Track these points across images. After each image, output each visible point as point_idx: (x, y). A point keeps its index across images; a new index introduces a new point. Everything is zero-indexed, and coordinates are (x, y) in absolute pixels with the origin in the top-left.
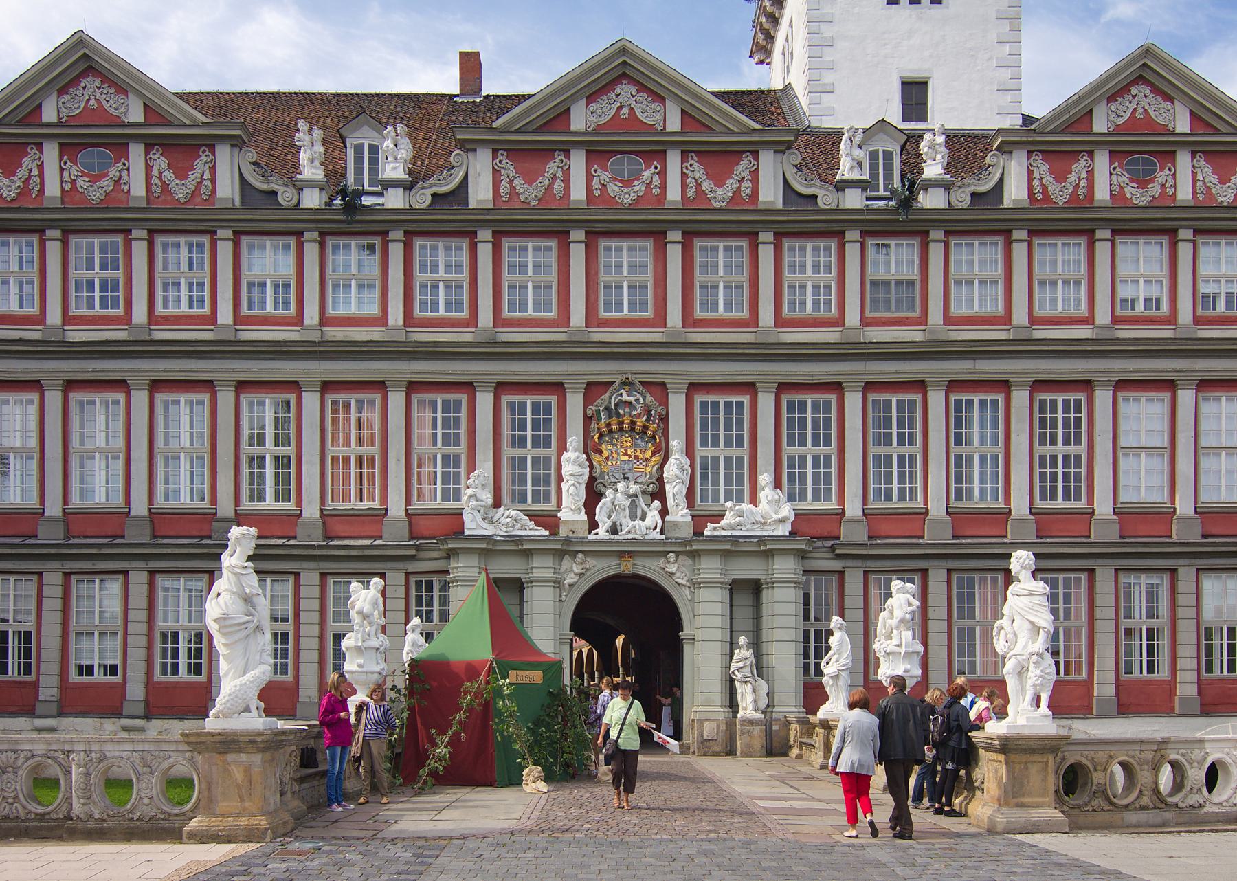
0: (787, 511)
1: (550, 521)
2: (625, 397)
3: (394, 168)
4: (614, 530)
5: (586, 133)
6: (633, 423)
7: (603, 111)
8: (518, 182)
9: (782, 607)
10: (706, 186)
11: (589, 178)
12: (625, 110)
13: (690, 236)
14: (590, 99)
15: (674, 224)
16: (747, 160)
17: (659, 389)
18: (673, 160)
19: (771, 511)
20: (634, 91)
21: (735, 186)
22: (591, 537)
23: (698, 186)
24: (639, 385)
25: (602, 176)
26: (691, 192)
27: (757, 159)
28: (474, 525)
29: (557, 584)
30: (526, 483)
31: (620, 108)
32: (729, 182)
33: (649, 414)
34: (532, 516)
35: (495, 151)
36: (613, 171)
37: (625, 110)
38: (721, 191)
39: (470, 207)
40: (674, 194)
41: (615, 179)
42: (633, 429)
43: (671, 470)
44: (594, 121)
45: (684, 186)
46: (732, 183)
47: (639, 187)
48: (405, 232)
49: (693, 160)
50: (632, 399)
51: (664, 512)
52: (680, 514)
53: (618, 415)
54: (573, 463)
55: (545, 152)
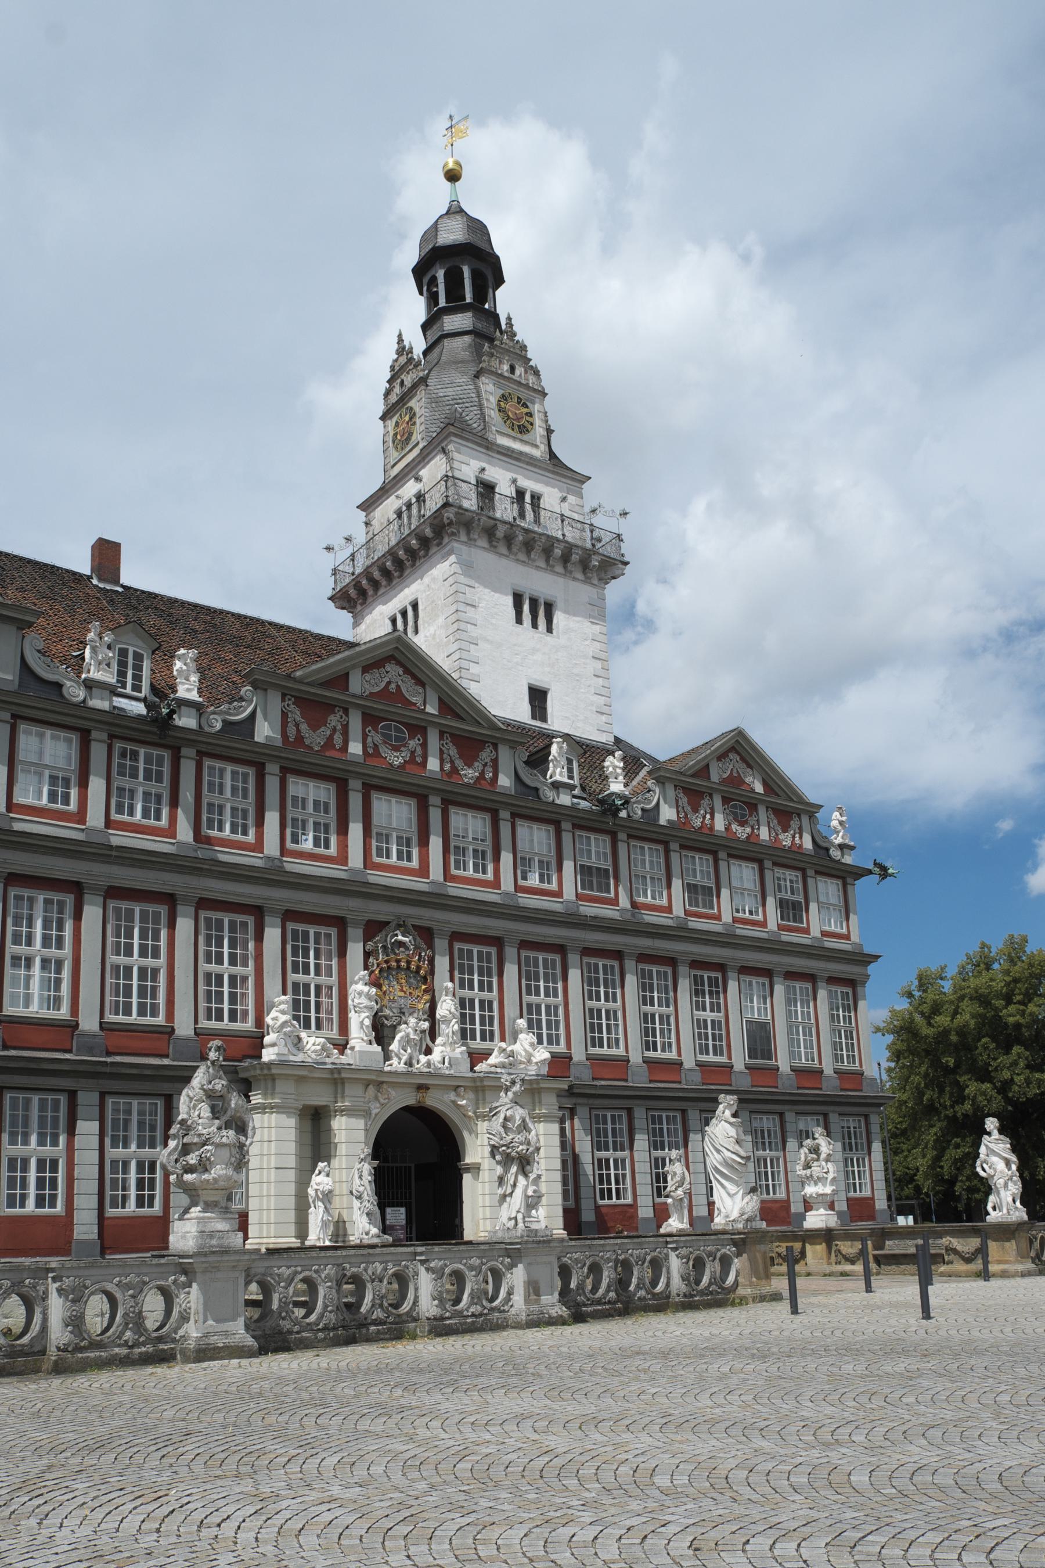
0: (542, 1054)
2: (400, 937)
3: (188, 690)
6: (408, 963)
8: (304, 727)
10: (459, 763)
13: (447, 803)
14: (366, 669)
15: (437, 791)
19: (529, 1051)
20: (401, 673)
22: (387, 1069)
26: (447, 767)
31: (389, 683)
32: (476, 764)
33: (420, 956)
35: (284, 696)
36: (383, 734)
37: (393, 686)
39: (256, 739)
41: (385, 742)
42: (408, 968)
48: (198, 751)
53: (395, 954)
55: (329, 707)
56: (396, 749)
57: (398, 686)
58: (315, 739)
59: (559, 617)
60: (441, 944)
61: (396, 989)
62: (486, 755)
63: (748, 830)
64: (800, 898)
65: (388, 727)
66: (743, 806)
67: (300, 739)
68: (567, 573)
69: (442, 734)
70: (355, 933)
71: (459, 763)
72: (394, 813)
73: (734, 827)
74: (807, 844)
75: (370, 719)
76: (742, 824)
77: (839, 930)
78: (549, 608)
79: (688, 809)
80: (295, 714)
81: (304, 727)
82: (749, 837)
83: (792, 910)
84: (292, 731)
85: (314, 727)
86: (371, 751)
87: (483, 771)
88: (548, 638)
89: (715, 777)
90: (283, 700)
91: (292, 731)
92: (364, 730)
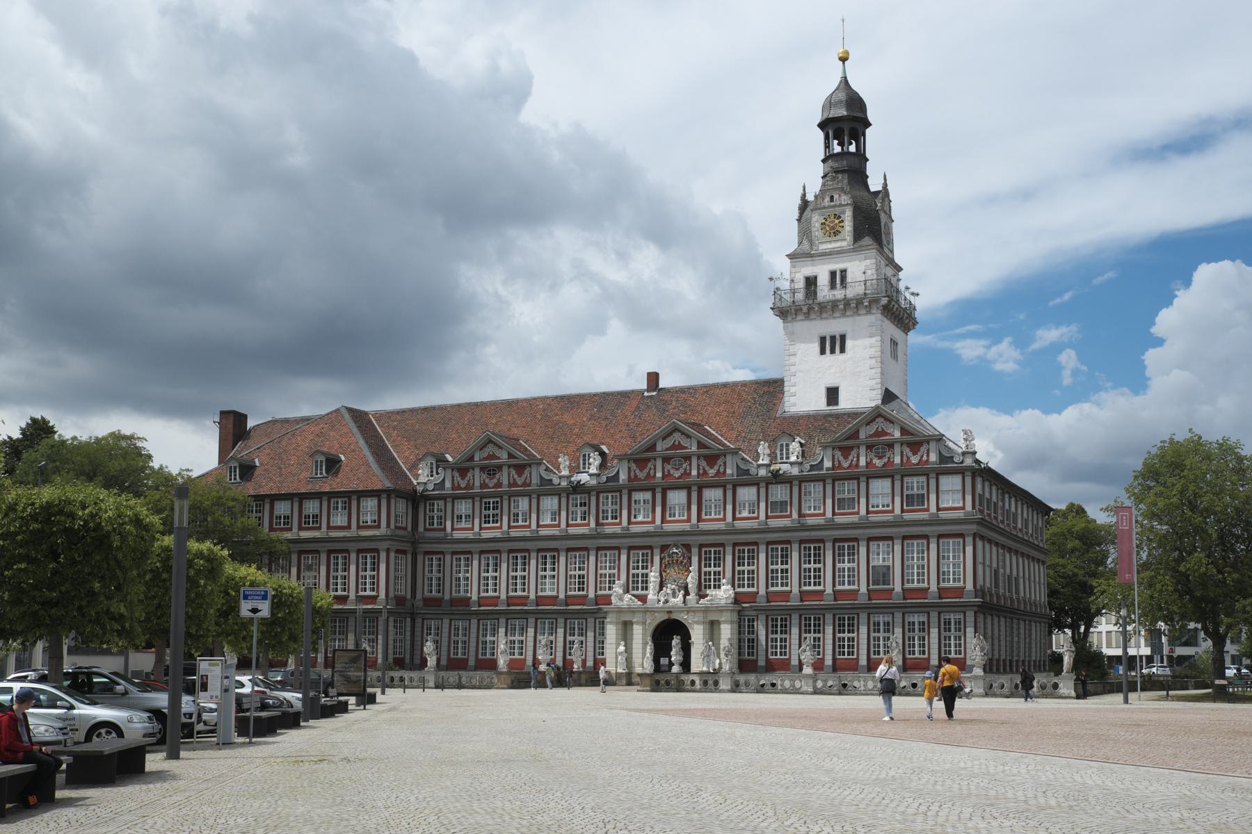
1: (643, 599)
4: (666, 601)
9: (726, 632)
10: (707, 468)
14: (664, 439)
18: (694, 461)
19: (723, 594)
25: (668, 467)
29: (644, 623)
30: (636, 584)
43: (689, 579)
44: (665, 447)
46: (716, 467)
51: (687, 593)
52: (692, 597)
54: (653, 576)
55: (648, 460)
58: (641, 475)
59: (849, 343)
60: (695, 551)
61: (672, 572)
62: (720, 462)
63: (886, 460)
64: (925, 492)
66: (879, 446)
67: (636, 476)
68: (857, 313)
69: (698, 458)
70: (657, 552)
71: (707, 468)
72: (677, 498)
73: (877, 462)
74: (933, 457)
76: (880, 458)
77: (956, 505)
78: (843, 338)
79: (841, 458)
80: (634, 466)
82: (885, 465)
83: (914, 501)
84: (632, 474)
85: (641, 470)
88: (843, 356)
89: (862, 435)
91: (632, 474)
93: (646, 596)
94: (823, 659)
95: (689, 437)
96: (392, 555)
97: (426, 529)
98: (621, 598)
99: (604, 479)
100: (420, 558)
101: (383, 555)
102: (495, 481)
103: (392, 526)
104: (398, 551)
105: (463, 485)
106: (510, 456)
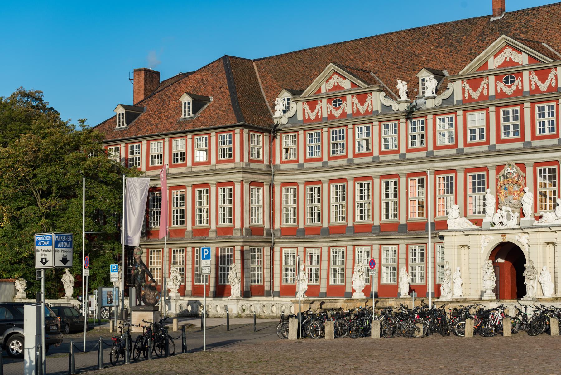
2: (509, 171)
5: (494, 70)
7: (500, 60)
10: (539, 83)
11: (496, 86)
12: (508, 60)
14: (495, 56)
16: (553, 71)
17: (522, 166)
21: (549, 83)
23: (536, 84)
24: (515, 166)
25: (501, 85)
26: (533, 87)
27: (556, 70)
28: (451, 225)
31: (506, 58)
32: (547, 81)
34: (472, 221)
38: (543, 85)
40: (526, 89)
41: (505, 85)
45: (530, 85)
47: (514, 88)
49: (533, 73)
50: (512, 171)
55: (481, 78)
56: (510, 87)
57: (510, 58)
58: (475, 95)
65: (507, 78)
67: (470, 96)
71: (539, 83)
75: (498, 77)
80: (467, 87)
81: (471, 91)
84: (466, 95)
85: (475, 90)
86: (499, 91)
87: (551, 83)
90: (463, 83)
91: (466, 95)
92: (496, 82)
93: (482, 220)
94: (185, 286)
95: (520, 51)
96: (246, 186)
97: (282, 162)
98: (455, 220)
99: (438, 101)
100: (277, 189)
101: (238, 187)
102: (340, 111)
103: (246, 159)
104: (252, 183)
105: (313, 117)
106: (354, 85)
